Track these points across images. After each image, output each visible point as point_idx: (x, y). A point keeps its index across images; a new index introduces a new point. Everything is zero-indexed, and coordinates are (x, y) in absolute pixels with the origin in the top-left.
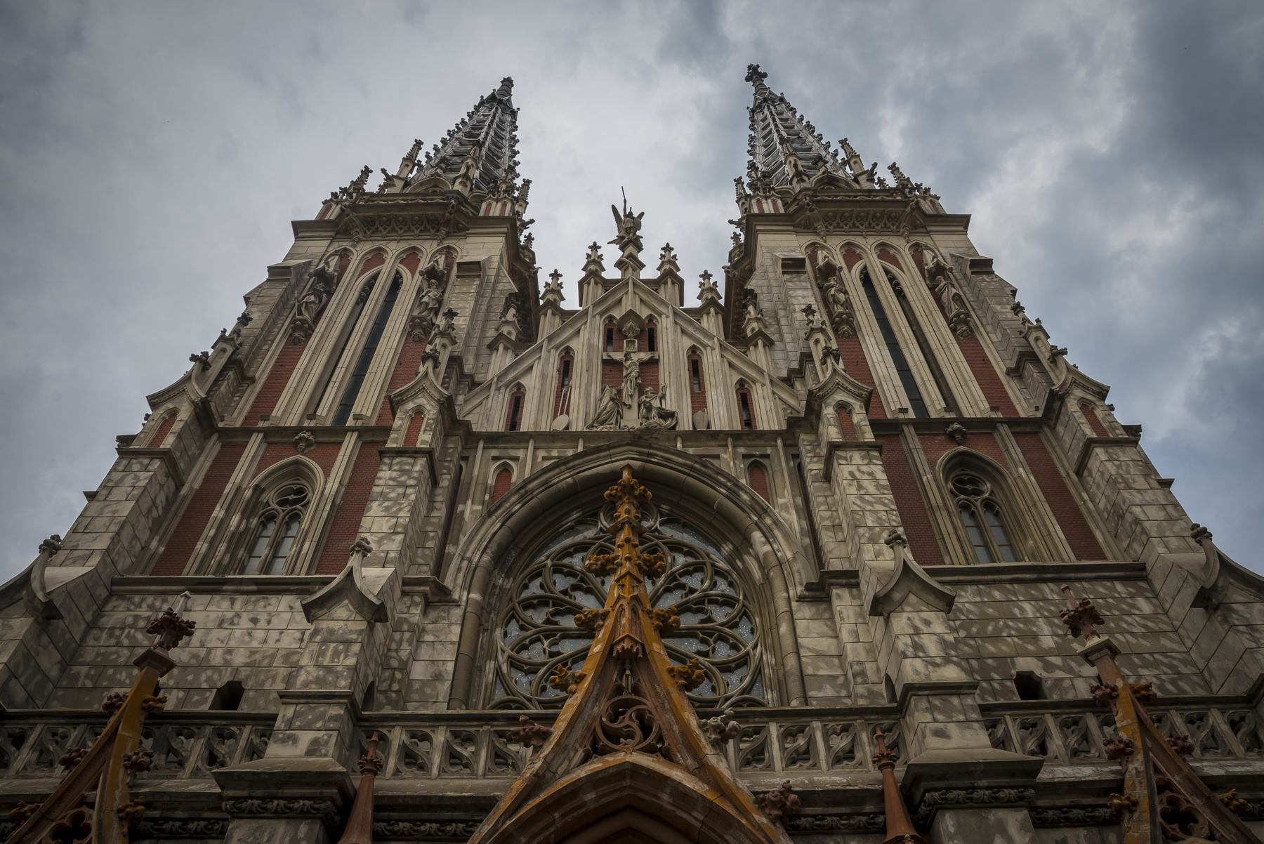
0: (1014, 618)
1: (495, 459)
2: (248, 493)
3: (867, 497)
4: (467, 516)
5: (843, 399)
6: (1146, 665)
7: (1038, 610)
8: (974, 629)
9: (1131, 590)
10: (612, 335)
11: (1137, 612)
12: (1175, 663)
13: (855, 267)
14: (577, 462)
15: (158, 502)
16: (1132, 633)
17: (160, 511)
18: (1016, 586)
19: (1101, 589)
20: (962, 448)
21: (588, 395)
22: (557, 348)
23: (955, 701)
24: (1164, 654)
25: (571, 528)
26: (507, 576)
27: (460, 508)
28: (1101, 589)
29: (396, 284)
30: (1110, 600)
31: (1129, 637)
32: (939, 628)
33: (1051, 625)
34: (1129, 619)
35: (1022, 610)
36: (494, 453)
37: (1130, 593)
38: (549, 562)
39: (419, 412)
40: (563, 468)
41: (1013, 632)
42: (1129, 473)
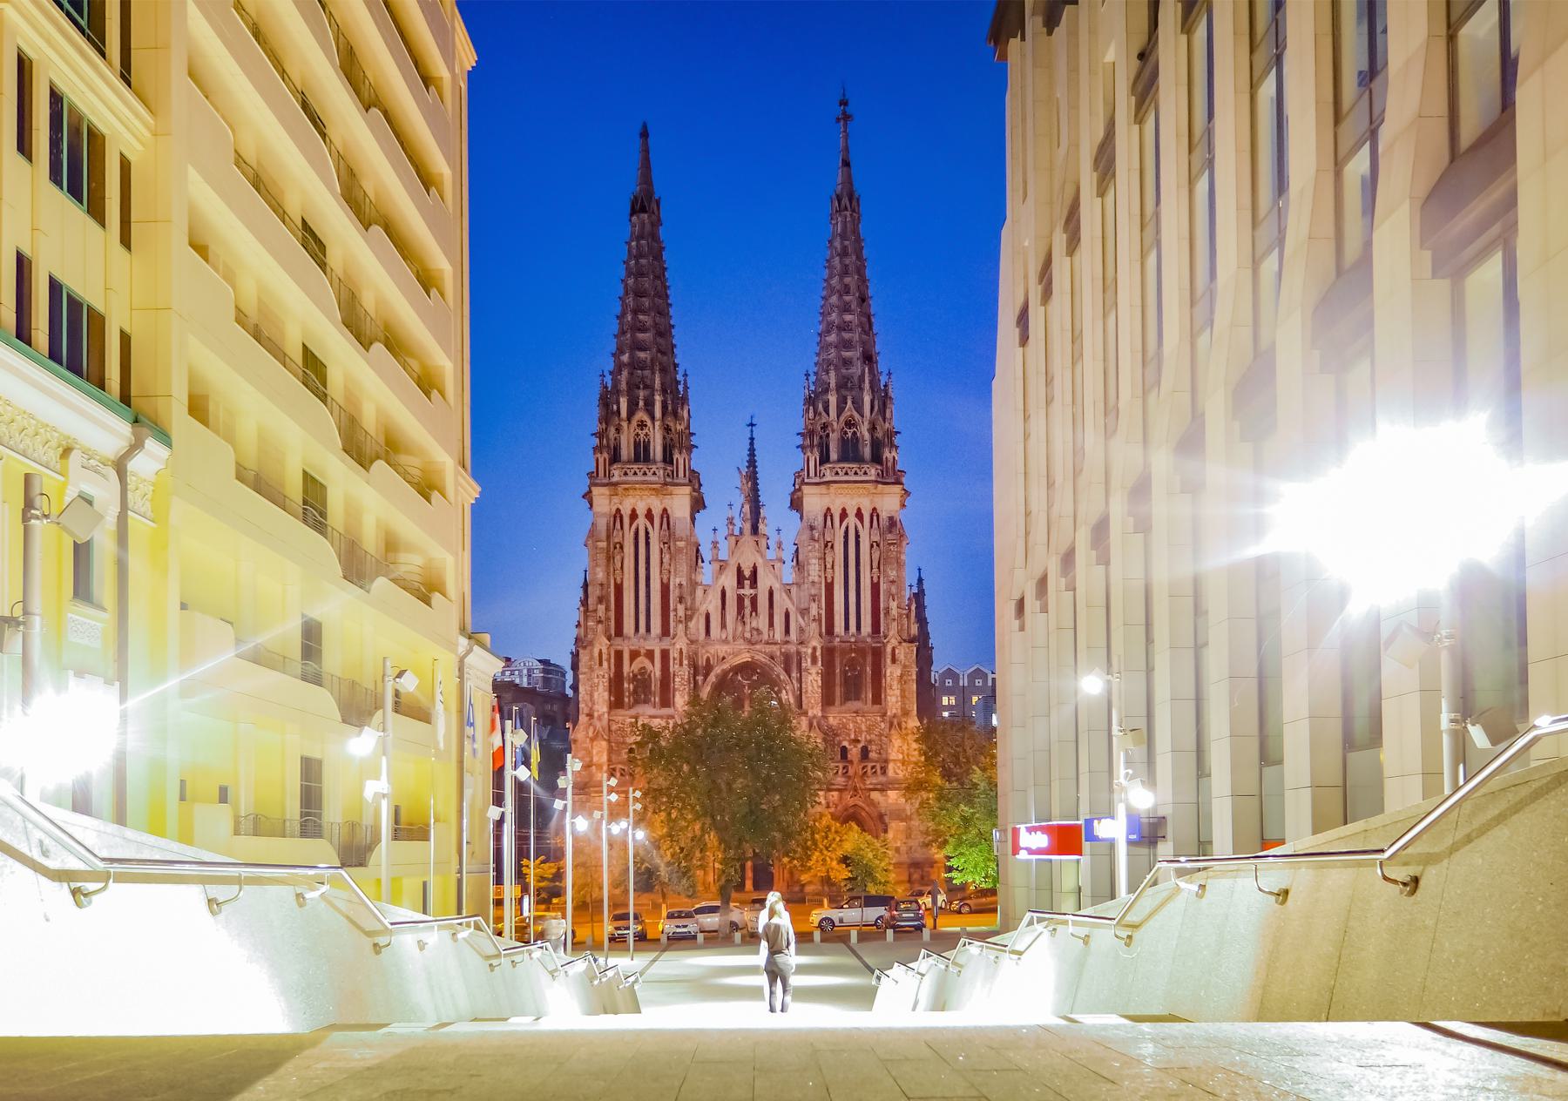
2: (631, 674)
4: (700, 683)
6: (876, 745)
20: (853, 655)
27: (697, 678)
29: (647, 533)
39: (681, 649)
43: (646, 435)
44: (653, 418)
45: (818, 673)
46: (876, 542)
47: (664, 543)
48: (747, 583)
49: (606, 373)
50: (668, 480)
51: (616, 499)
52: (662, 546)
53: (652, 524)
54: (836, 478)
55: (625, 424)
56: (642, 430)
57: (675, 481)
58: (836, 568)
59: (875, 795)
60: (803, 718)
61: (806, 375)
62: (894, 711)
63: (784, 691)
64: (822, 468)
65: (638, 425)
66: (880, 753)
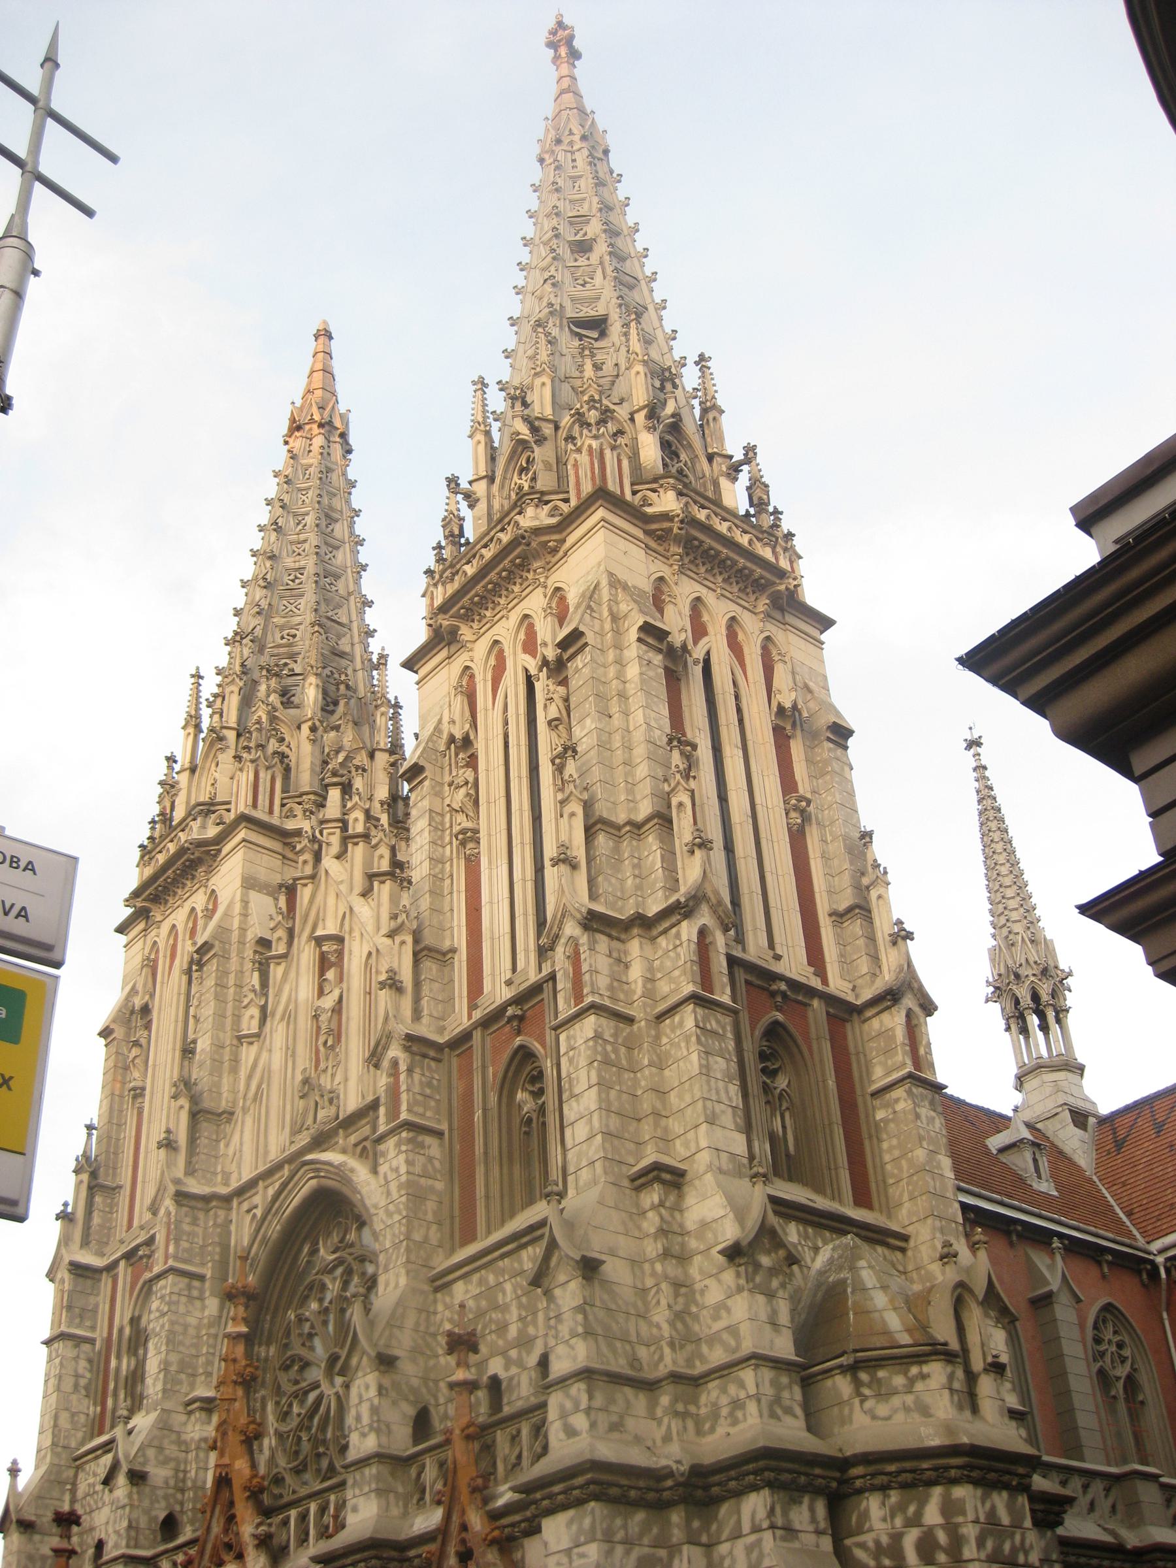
0: (496, 1307)
1: (248, 1211)
2: (127, 1331)
10: (324, 964)
14: (277, 1205)
15: (81, 1371)
17: (88, 1375)
20: (518, 1041)
22: (282, 1019)
25: (308, 1262)
26: (268, 1344)
33: (521, 1306)
35: (504, 1293)
36: (245, 1206)
38: (293, 1317)
40: (269, 1217)
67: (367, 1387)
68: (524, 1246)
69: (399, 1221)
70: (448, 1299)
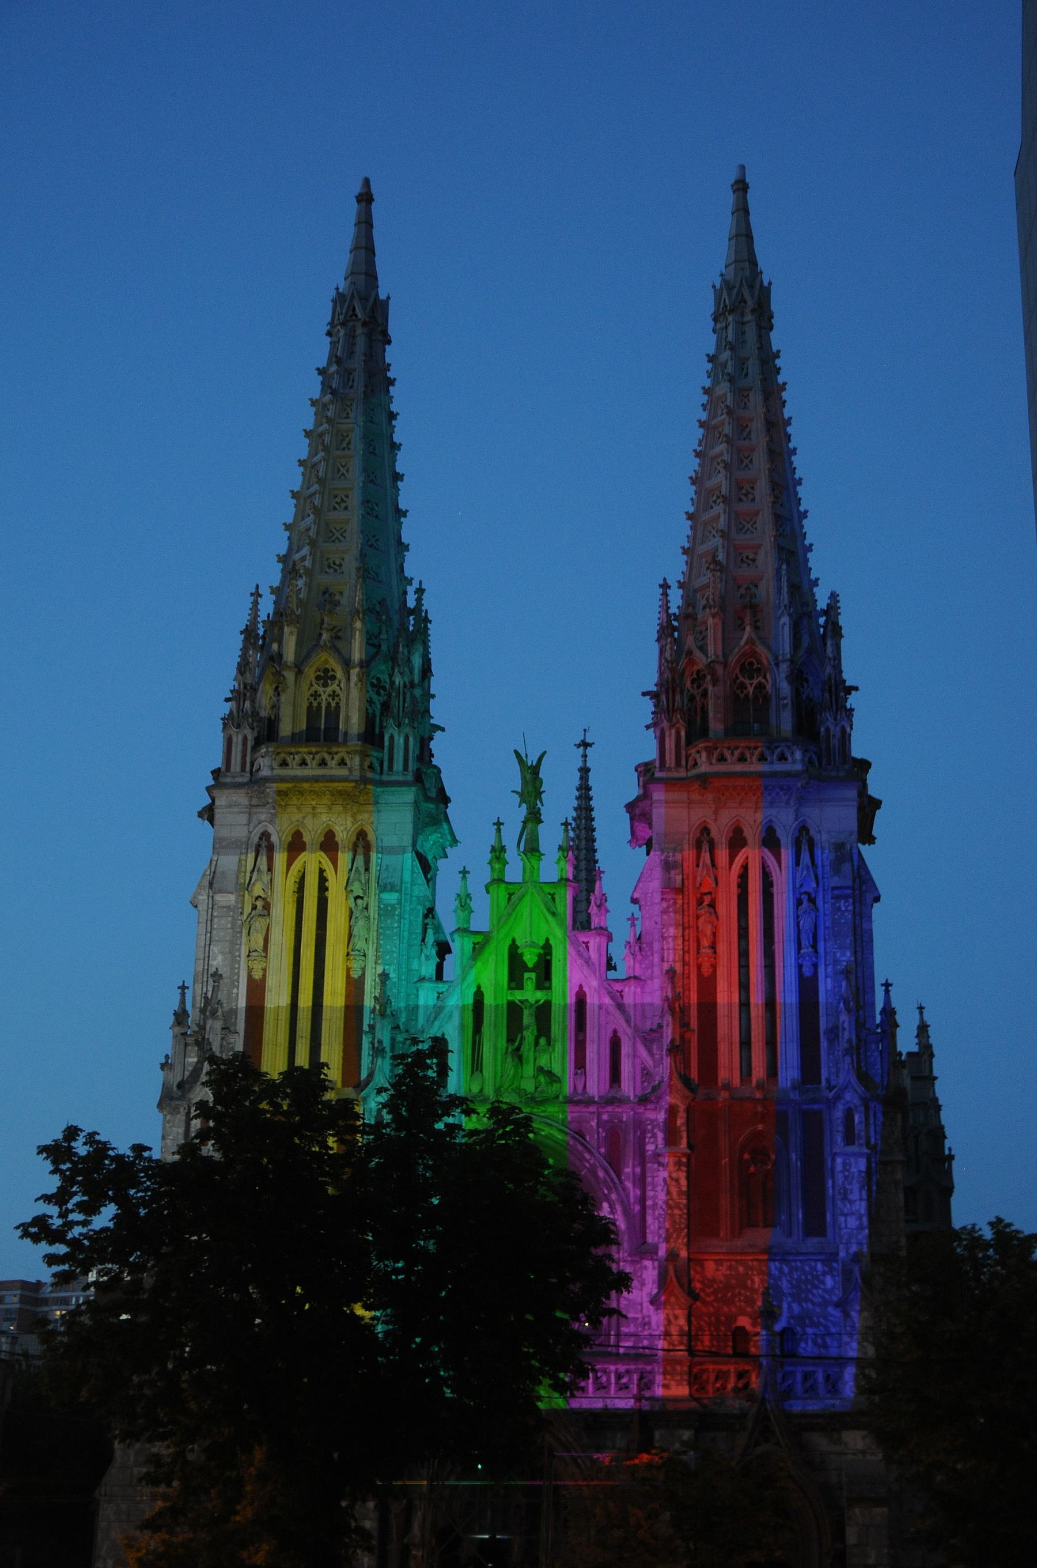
3: (670, 1202)
5: (673, 1101)
7: (762, 1281)
8: (720, 1295)
9: (826, 1269)
11: (822, 1287)
12: (829, 1324)
13: (737, 859)
16: (813, 1303)
18: (754, 1263)
19: (807, 1268)
20: (760, 1127)
21: (496, 1049)
23: (678, 1368)
24: (825, 1318)
28: (807, 1268)
29: (323, 880)
30: (809, 1277)
31: (810, 1306)
32: (682, 1322)
34: (815, 1291)
35: (753, 1281)
37: (824, 1271)
41: (742, 1298)
42: (851, 1183)
43: (334, 695)
44: (347, 664)
45: (679, 1164)
46: (808, 894)
47: (357, 898)
48: (530, 978)
49: (265, 591)
50: (370, 775)
51: (263, 815)
52: (353, 905)
53: (334, 862)
54: (721, 768)
55: (290, 676)
56: (325, 685)
57: (385, 778)
58: (722, 948)
59: (819, 1441)
60: (648, 1263)
61: (661, 586)
62: (854, 1248)
63: (605, 1205)
64: (693, 751)
65: (318, 678)
66: (825, 1346)
67: (676, 1317)
68: (774, 1260)
69: (680, 1215)
70: (698, 1269)
